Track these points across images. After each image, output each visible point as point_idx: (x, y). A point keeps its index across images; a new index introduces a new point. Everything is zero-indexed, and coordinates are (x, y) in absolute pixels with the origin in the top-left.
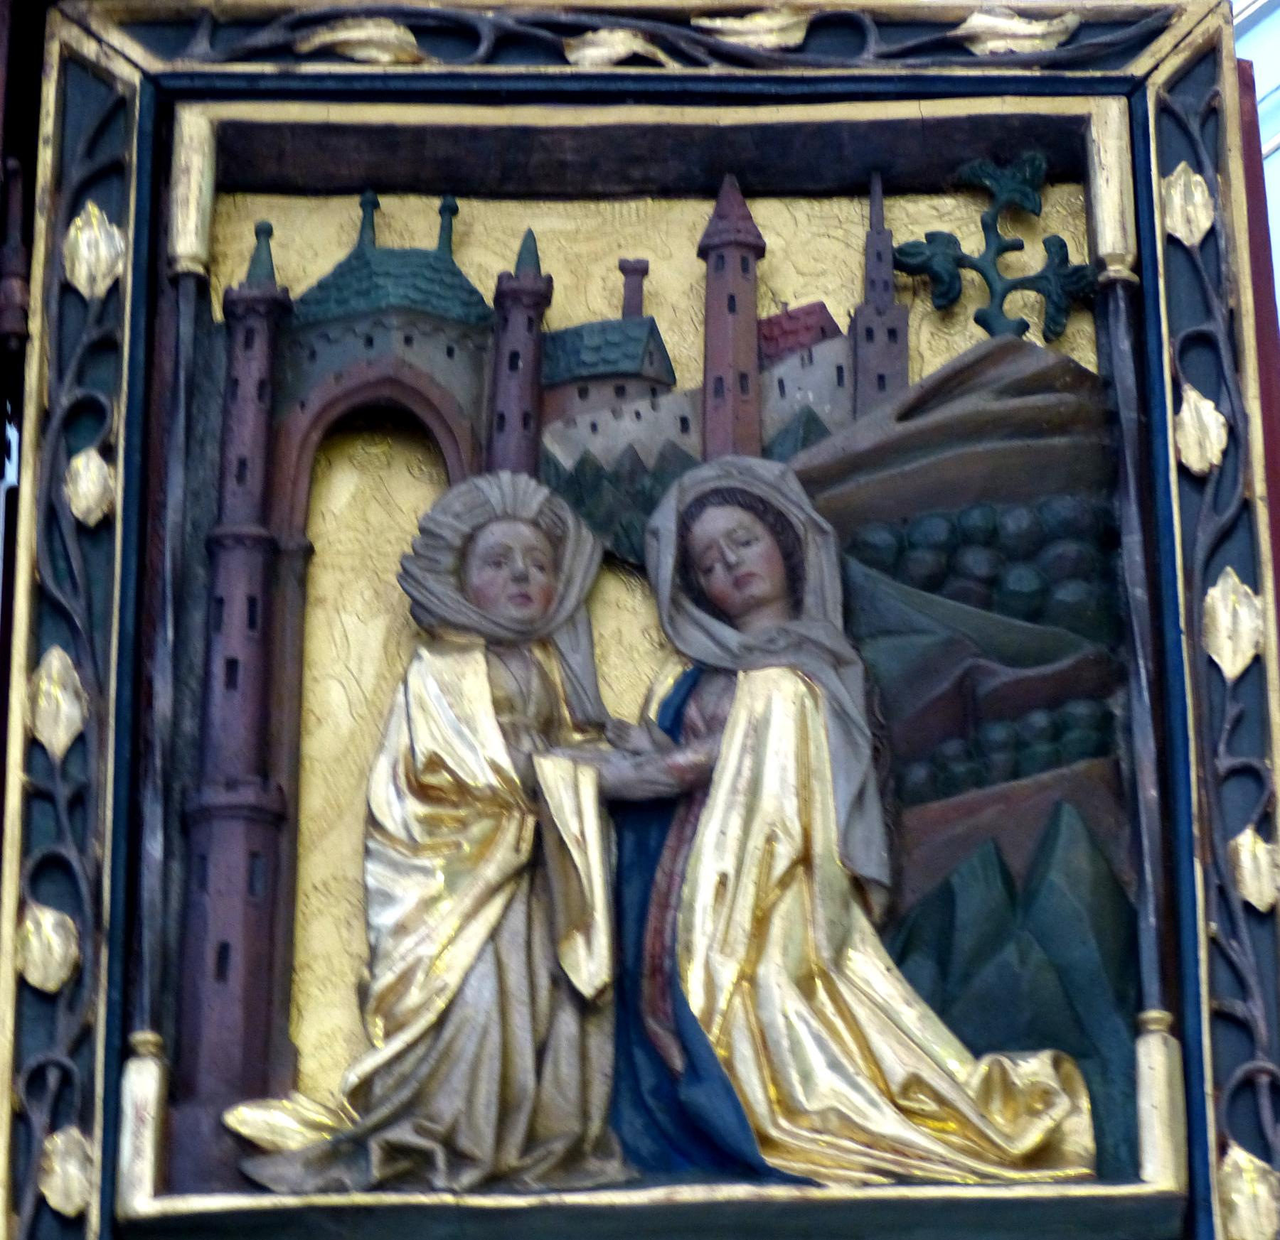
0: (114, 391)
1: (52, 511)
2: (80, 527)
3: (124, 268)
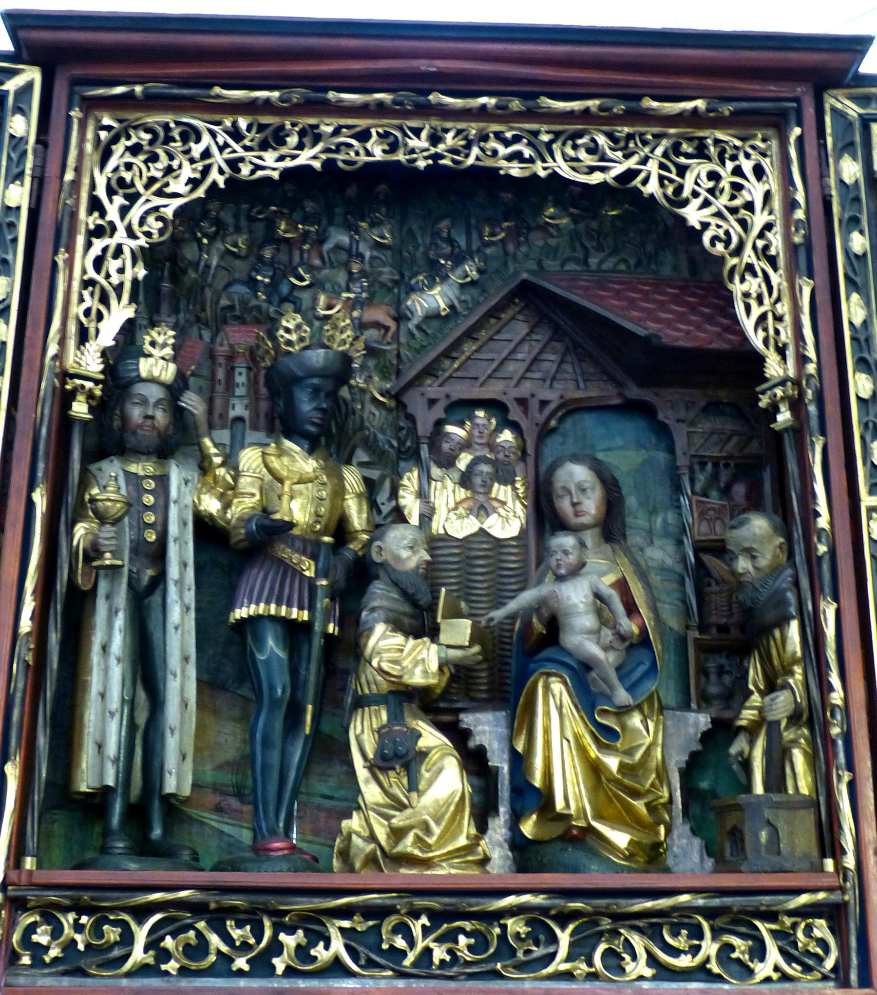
0: (860, 212)
1: (847, 252)
2: (856, 256)
3: (860, 175)
